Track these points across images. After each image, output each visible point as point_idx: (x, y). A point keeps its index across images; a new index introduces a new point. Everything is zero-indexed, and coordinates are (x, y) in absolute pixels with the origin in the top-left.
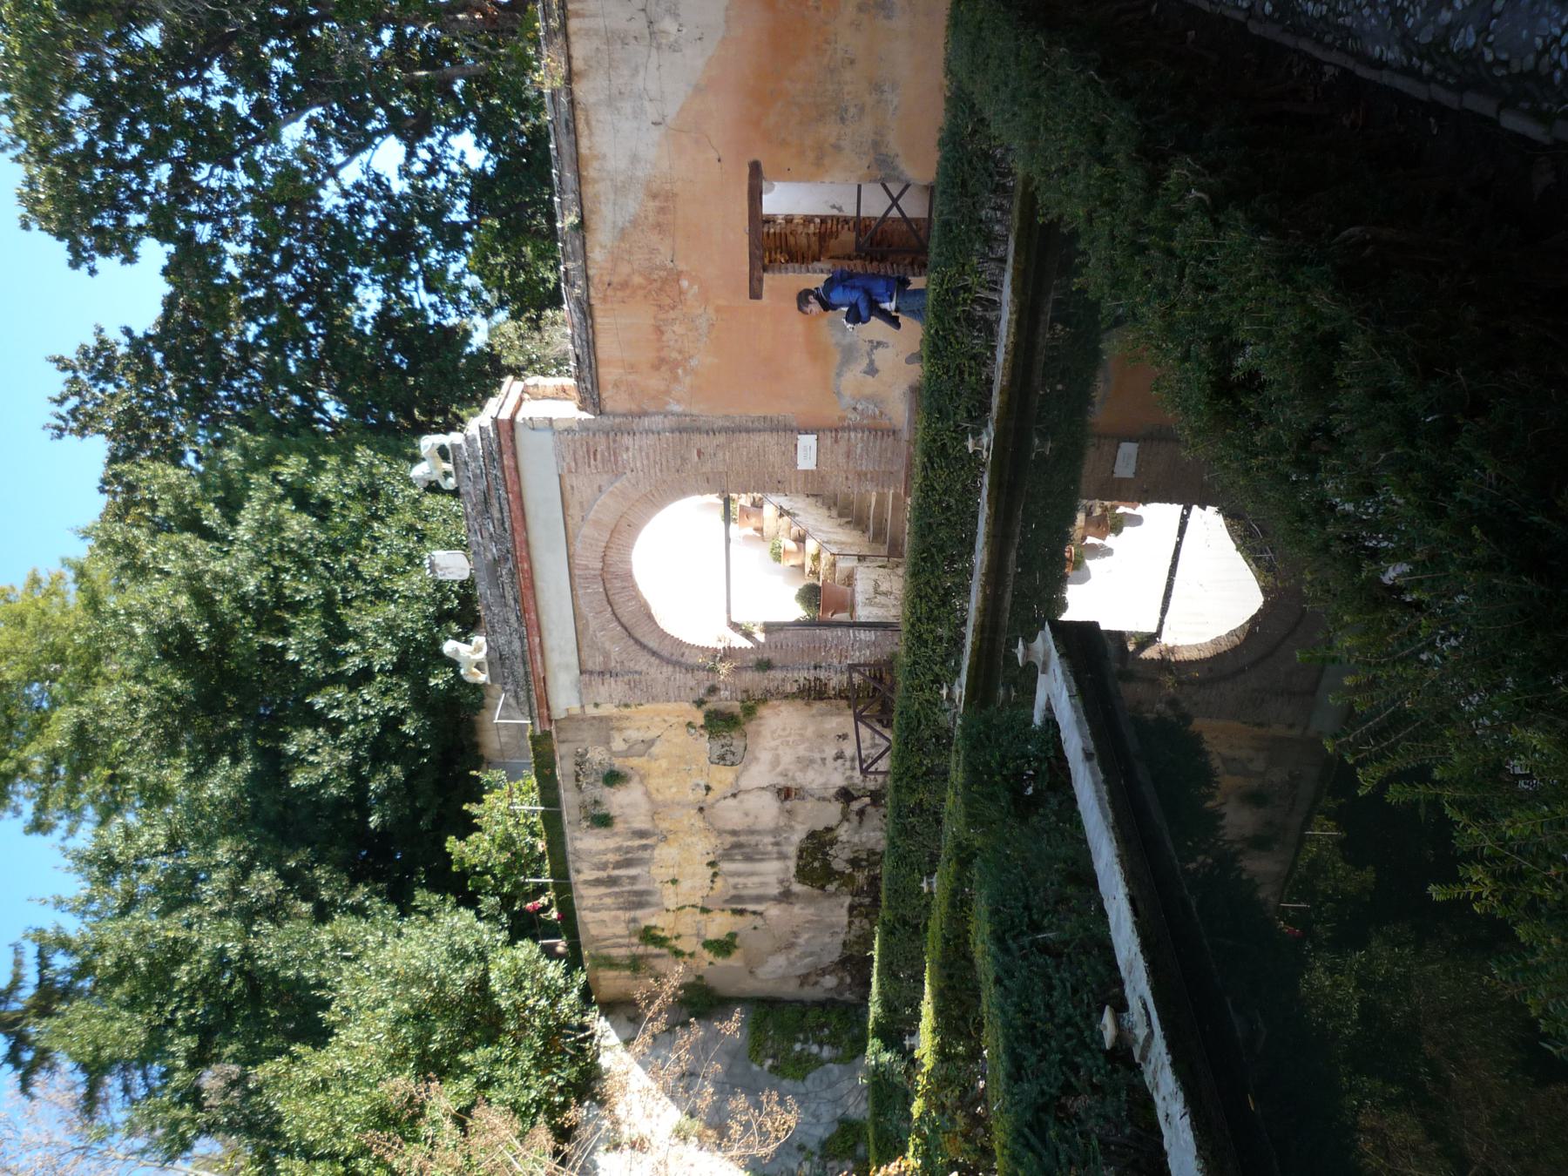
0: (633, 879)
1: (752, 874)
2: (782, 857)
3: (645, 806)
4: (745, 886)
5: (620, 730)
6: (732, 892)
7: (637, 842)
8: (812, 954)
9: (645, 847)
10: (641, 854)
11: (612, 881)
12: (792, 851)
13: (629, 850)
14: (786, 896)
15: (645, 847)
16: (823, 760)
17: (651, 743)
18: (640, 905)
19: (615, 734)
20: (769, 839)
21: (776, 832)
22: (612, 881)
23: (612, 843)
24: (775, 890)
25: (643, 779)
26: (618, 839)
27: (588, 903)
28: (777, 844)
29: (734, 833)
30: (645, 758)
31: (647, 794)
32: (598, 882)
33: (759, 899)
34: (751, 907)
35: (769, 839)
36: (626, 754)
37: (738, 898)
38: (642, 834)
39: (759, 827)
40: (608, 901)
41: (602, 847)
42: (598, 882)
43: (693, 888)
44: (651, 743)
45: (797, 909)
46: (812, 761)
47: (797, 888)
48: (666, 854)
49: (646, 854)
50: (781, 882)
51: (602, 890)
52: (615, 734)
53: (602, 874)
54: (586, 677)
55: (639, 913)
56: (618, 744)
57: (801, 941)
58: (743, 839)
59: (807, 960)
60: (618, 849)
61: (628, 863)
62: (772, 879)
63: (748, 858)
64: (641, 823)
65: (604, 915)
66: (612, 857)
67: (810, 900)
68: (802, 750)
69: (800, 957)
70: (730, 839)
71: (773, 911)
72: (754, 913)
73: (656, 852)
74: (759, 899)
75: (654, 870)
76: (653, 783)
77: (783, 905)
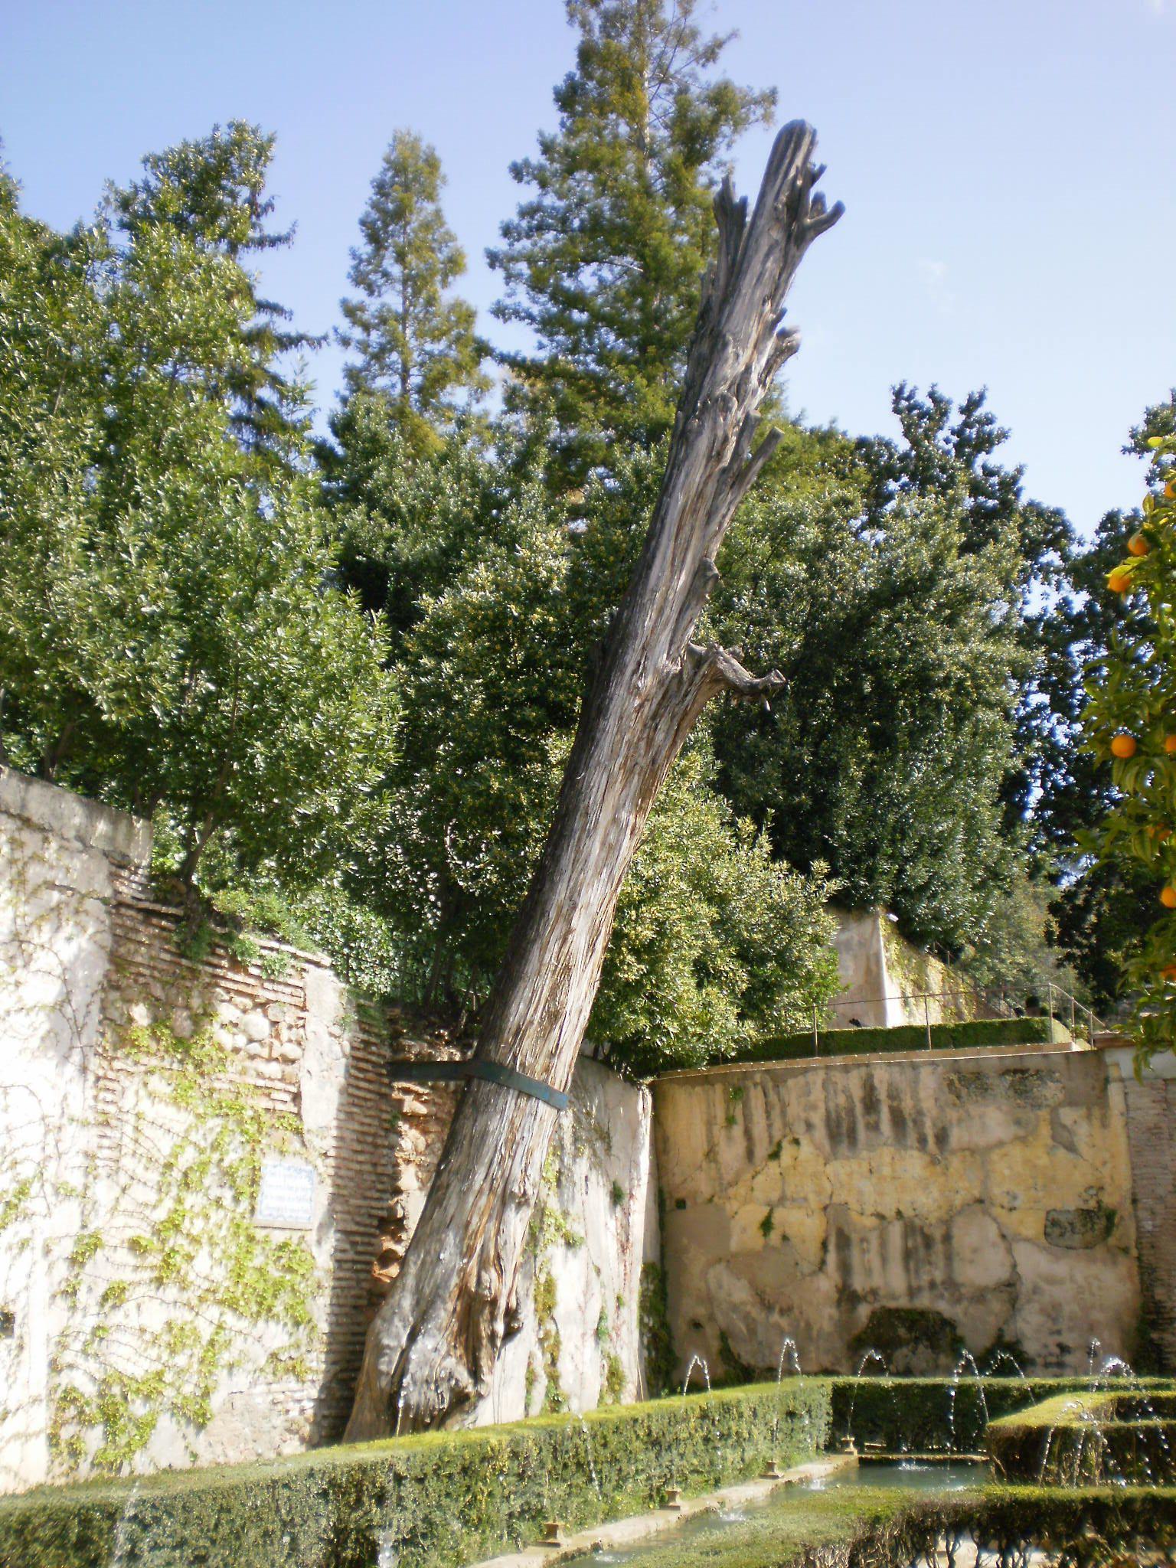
0: (874, 1127)
1: (884, 1260)
2: (912, 1292)
3: (981, 1141)
4: (864, 1252)
5: (1089, 1117)
6: (855, 1237)
7: (930, 1132)
8: (752, 1331)
9: (922, 1141)
10: (912, 1138)
11: (871, 1104)
12: (924, 1301)
13: (918, 1123)
14: (848, 1297)
15: (922, 1141)
16: (1059, 1332)
17: (1071, 1148)
18: (834, 1136)
19: (1082, 1111)
20: (939, 1276)
21: (951, 1284)
22: (871, 1104)
23: (928, 1105)
24: (858, 1284)
25: (1022, 1140)
26: (935, 1112)
27: (838, 1077)
28: (932, 1285)
29: (947, 1238)
30: (1050, 1142)
31: (1000, 1144)
32: (869, 1088)
33: (845, 1268)
34: (832, 1258)
35: (939, 1276)
36: (1055, 1123)
37: (844, 1242)
38: (942, 1138)
39: (956, 1264)
40: (841, 1100)
41: (922, 1095)
42: (869, 1088)
43: (860, 1193)
44: (1071, 1148)
45: (831, 1311)
46: (1055, 1320)
48: (914, 1163)
49: (912, 1138)
50: (874, 1292)
51: (858, 1093)
52: (1082, 1111)
53: (882, 1094)
54: (1160, 1083)
55: (820, 1133)
56: (1068, 1115)
57: (775, 1317)
58: (939, 1247)
59: (742, 1326)
60: (920, 1113)
61: (898, 1120)
62: (877, 1281)
63: (908, 1255)
64: (956, 1136)
65: (817, 1094)
66: (907, 1105)
67: (844, 1325)
68: (1070, 1308)
69: (746, 1317)
70: (937, 1234)
71: (827, 1284)
72: (823, 1262)
73: (916, 1153)
74: (845, 1268)
75: (886, 1154)
76: (1017, 1152)
77: (836, 1296)
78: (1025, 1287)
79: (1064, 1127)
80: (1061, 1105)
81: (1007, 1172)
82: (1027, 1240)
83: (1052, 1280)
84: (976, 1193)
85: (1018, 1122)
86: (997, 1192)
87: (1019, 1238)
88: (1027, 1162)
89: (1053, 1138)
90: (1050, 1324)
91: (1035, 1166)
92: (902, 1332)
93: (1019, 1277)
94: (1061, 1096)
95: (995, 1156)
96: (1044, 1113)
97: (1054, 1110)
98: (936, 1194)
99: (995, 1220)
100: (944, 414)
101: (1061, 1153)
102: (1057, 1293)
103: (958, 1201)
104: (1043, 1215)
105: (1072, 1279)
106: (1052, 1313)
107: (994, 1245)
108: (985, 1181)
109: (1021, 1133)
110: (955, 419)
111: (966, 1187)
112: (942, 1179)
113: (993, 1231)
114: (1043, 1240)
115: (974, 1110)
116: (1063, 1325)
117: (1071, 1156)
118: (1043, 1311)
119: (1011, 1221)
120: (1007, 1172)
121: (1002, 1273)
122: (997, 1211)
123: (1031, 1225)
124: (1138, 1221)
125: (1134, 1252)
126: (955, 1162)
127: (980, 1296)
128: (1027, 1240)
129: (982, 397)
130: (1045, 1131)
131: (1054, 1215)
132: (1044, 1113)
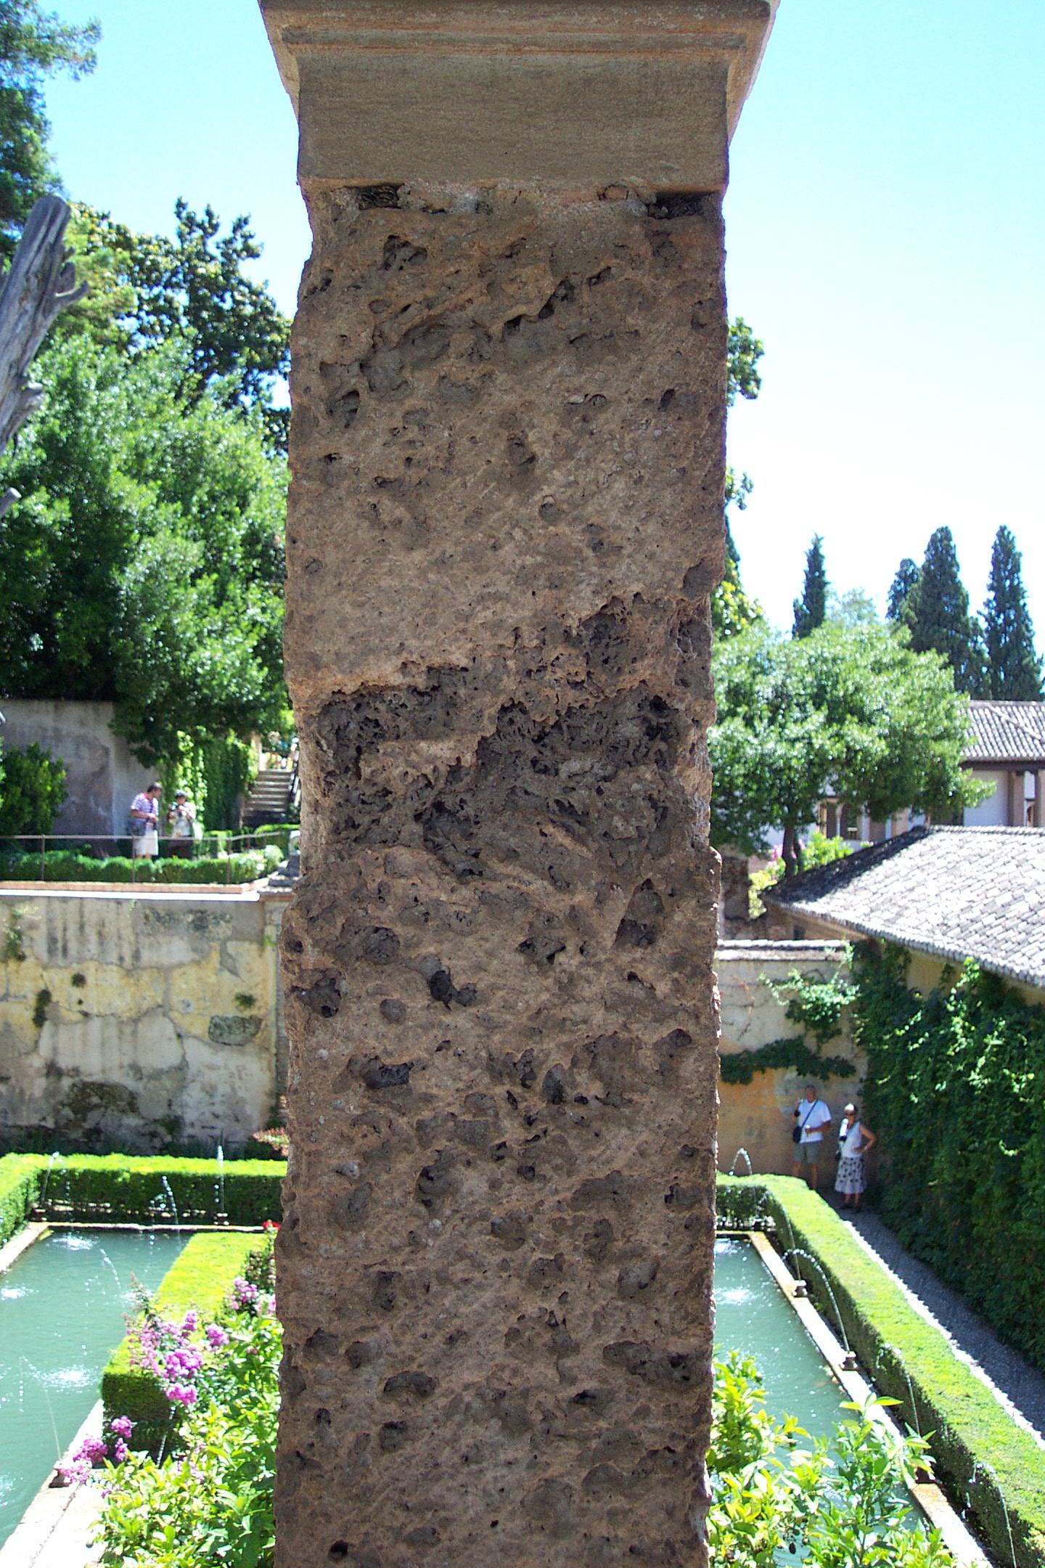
3: (166, 961)
25: (198, 963)
30: (218, 966)
31: (181, 965)
36: (223, 951)
46: (211, 1096)
47: (66, 1082)
50: (76, 1071)
64: (146, 956)
68: (223, 1089)
76: (193, 972)
78: (193, 1069)
79: (230, 956)
80: (229, 939)
81: (184, 986)
82: (195, 1037)
83: (212, 1067)
84: (160, 1001)
85: (194, 950)
86: (175, 1000)
87: (190, 1036)
88: (199, 979)
89: (221, 963)
90: (207, 1098)
91: (206, 983)
92: (95, 1100)
93: (187, 1065)
94: (229, 933)
95: (176, 973)
96: (215, 944)
97: (224, 943)
98: (129, 999)
99: (172, 1020)
100: (215, 227)
101: (226, 974)
102: (212, 1077)
103: (145, 1006)
104: (208, 1019)
105: (226, 1067)
106: (210, 1091)
107: (170, 1039)
108: (167, 993)
109: (197, 957)
110: (225, 232)
111: (152, 995)
112: (133, 989)
113: (170, 1031)
114: (207, 1038)
115: (162, 939)
116: (218, 1099)
117: (234, 977)
118: (203, 1089)
119: (185, 1023)
120: (184, 986)
121: (174, 1060)
122: (174, 1015)
123: (200, 1027)
124: (278, 1029)
125: (274, 1051)
126: (146, 977)
127: (157, 1075)
128: (195, 1037)
129: (246, 222)
130: (215, 957)
131: (218, 1020)
132: (215, 944)
